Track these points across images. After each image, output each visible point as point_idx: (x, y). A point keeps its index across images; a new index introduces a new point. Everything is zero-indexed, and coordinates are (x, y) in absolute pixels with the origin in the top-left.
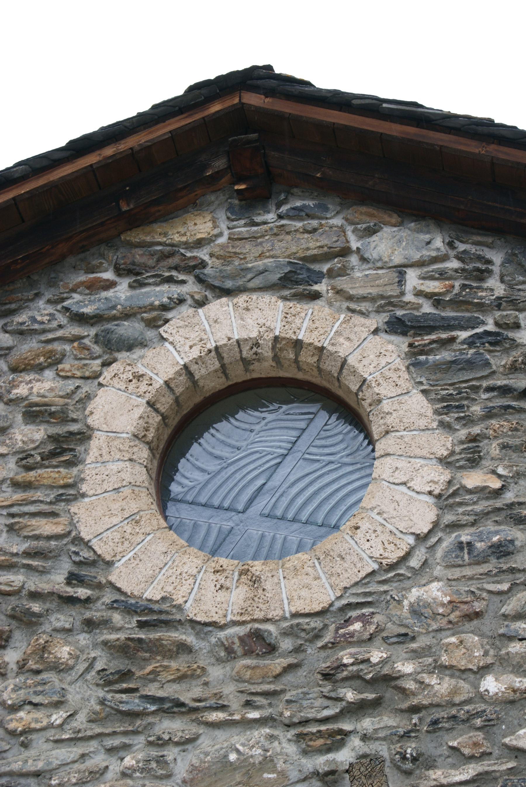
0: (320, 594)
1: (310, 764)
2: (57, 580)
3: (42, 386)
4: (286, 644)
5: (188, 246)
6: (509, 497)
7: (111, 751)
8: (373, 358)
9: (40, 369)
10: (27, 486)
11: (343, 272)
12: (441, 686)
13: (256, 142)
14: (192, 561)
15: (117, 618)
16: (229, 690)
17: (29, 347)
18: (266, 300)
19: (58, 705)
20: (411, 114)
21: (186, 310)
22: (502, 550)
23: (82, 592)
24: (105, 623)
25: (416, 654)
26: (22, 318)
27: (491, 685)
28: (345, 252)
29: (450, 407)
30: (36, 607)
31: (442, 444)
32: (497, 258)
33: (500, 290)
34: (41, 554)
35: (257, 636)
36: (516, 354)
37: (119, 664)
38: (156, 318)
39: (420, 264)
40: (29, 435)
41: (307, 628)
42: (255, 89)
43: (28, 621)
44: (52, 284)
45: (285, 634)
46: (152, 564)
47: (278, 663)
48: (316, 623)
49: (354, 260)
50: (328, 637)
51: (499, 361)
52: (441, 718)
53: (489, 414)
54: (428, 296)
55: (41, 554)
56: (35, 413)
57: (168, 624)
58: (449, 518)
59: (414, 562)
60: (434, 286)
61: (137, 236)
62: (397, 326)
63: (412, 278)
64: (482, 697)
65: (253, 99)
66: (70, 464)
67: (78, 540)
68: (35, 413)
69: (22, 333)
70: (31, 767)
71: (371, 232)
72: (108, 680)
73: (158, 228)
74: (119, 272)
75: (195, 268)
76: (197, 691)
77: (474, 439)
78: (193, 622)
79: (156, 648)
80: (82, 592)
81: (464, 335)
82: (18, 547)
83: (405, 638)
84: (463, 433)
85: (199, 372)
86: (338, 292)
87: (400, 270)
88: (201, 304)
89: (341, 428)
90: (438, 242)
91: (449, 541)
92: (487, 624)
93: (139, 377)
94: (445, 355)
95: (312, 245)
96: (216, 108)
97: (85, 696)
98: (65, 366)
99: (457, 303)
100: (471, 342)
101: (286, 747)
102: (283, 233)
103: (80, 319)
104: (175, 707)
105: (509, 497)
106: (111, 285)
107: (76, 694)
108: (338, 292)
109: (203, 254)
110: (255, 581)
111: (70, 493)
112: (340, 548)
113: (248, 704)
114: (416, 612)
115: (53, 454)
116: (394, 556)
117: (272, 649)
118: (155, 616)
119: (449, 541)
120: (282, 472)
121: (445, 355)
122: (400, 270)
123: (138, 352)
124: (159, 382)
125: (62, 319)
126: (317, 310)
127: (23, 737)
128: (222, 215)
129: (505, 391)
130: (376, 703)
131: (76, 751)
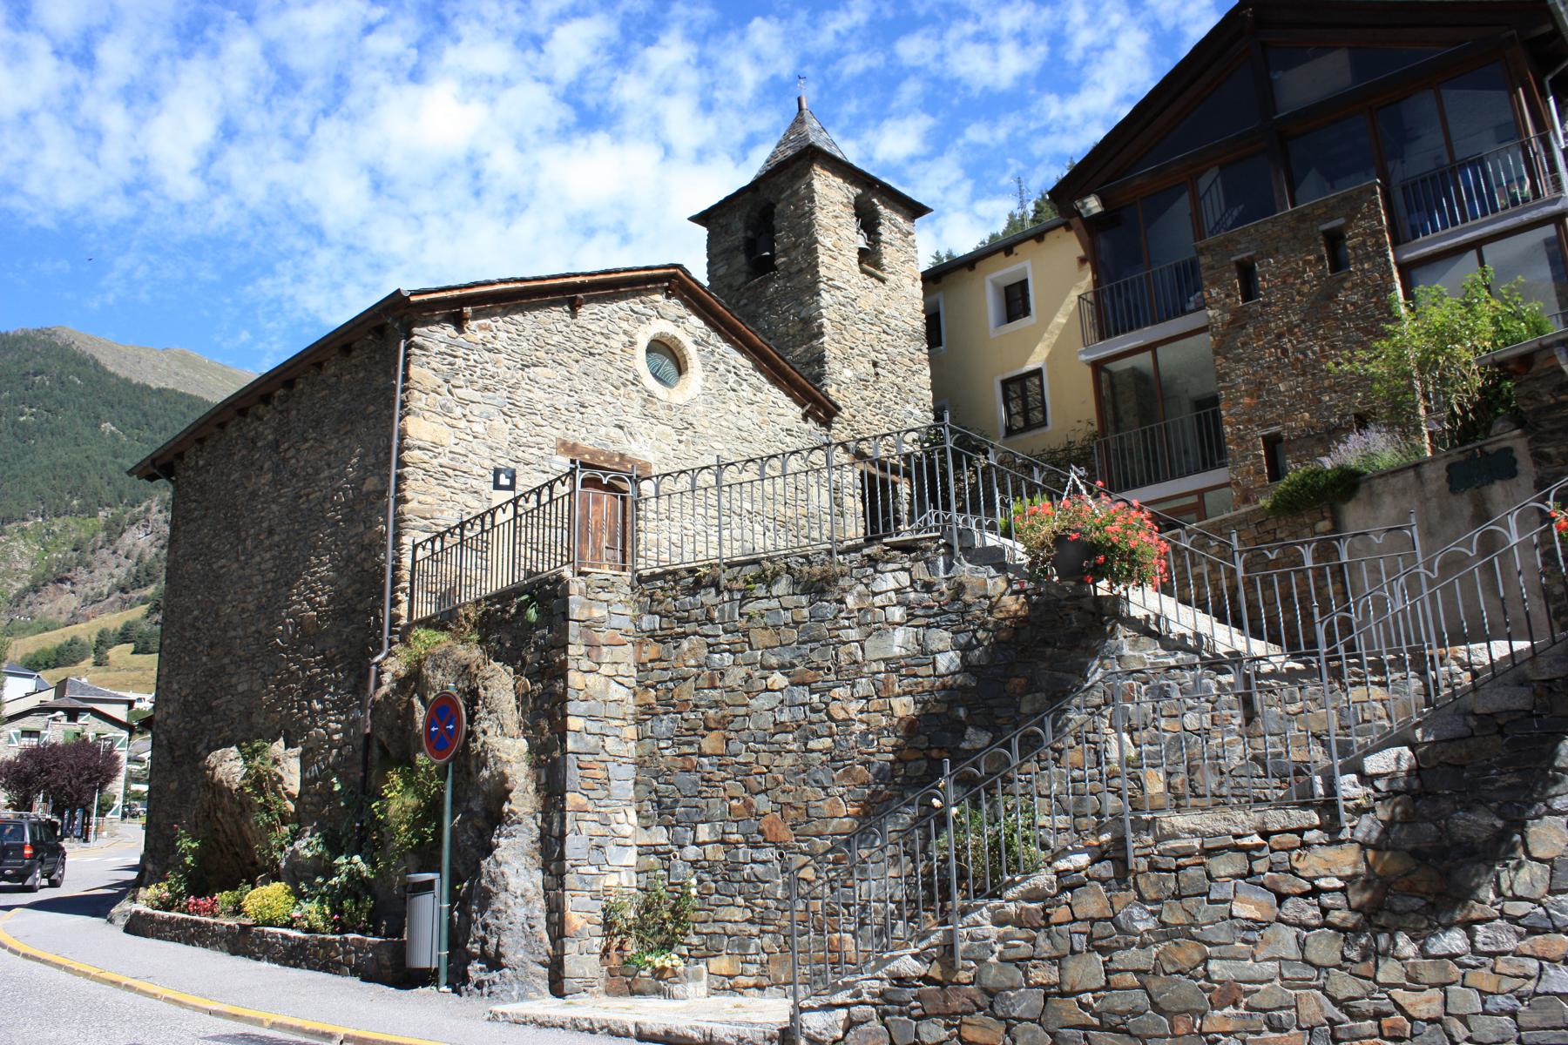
2: (631, 377)
8: (691, 350)
17: (622, 313)
29: (704, 365)
40: (626, 339)
55: (627, 370)
56: (625, 333)
62: (696, 342)
68: (625, 333)
97: (637, 409)
102: (674, 307)
104: (654, 417)
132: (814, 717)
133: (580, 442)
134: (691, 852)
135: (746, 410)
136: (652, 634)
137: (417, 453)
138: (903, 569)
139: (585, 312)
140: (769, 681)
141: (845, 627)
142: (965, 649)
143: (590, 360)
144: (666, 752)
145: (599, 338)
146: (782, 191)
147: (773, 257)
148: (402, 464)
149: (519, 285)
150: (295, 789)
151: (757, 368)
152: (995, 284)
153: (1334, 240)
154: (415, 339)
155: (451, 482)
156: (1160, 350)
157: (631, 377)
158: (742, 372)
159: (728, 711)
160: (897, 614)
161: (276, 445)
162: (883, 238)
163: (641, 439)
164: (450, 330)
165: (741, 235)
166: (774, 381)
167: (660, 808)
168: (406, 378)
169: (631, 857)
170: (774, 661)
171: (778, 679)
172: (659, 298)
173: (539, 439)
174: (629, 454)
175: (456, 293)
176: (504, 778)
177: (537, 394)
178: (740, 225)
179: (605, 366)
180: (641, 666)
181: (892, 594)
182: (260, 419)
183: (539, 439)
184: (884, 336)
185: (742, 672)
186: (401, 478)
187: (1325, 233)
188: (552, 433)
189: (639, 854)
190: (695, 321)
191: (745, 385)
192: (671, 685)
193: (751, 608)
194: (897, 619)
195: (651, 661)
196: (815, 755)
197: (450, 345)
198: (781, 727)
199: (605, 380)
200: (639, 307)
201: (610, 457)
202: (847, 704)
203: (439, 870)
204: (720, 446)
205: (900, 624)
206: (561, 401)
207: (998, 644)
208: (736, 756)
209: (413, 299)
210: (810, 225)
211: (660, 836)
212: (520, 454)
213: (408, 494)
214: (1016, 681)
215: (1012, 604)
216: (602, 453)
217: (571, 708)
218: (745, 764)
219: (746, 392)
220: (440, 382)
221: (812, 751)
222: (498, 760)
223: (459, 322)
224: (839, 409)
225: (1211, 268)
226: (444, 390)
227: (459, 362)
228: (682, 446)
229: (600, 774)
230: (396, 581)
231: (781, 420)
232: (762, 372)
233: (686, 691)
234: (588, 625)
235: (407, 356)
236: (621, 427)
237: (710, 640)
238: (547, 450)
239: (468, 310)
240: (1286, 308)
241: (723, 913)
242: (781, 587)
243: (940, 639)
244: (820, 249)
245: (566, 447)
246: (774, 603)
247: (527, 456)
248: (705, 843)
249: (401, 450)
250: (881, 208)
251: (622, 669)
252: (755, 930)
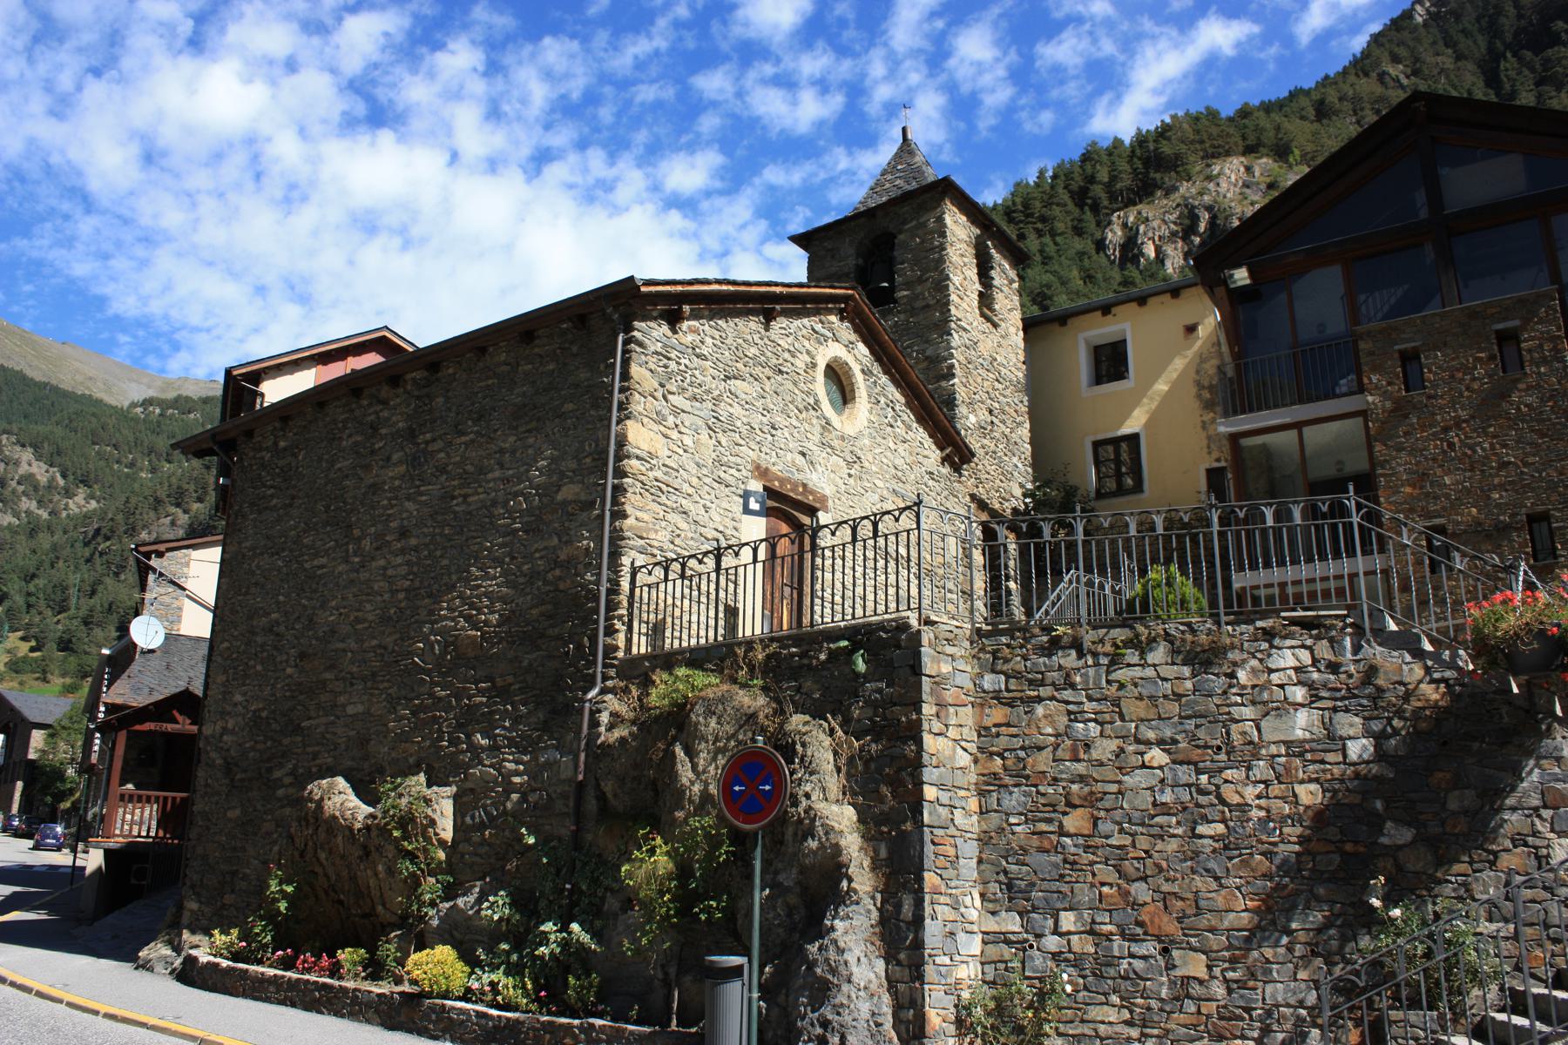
2: (812, 401)
8: (859, 378)
17: (804, 331)
40: (809, 360)
55: (808, 393)
56: (808, 352)
62: (863, 371)
68: (808, 352)
97: (816, 438)
132: (1203, 800)
134: (1052, 943)
135: (901, 448)
136: (997, 695)
137: (634, 462)
138: (1303, 646)
139: (780, 323)
140: (1147, 757)
141: (1237, 704)
142: (1379, 738)
143: (779, 378)
144: (1017, 829)
145: (786, 355)
146: (904, 223)
147: (892, 289)
148: (621, 473)
149: (731, 288)
150: (448, 835)
151: (908, 404)
152: (1087, 342)
153: (1507, 339)
154: (635, 333)
155: (663, 499)
156: (1307, 431)
157: (812, 401)
158: (897, 408)
159: (1099, 787)
160: (1299, 694)
161: (411, 434)
162: (996, 283)
164: (665, 329)
165: (852, 262)
166: (921, 420)
167: (1010, 891)
168: (626, 376)
169: (975, 946)
170: (1151, 735)
171: (1157, 756)
173: (739, 460)
174: (811, 485)
175: (680, 288)
176: (837, 850)
177: (737, 410)
178: (851, 251)
179: (791, 387)
180: (982, 731)
181: (1292, 672)
182: (385, 402)
183: (739, 460)
184: (997, 385)
185: (1113, 745)
186: (619, 490)
187: (1497, 332)
188: (749, 454)
189: (984, 942)
190: (862, 349)
192: (1022, 754)
193: (1121, 674)
194: (1299, 699)
195: (995, 725)
196: (1206, 841)
197: (665, 346)
198: (1165, 809)
200: (818, 327)
201: (795, 485)
202: (1242, 788)
203: (747, 952)
205: (1303, 705)
206: (757, 419)
207: (1417, 735)
208: (1107, 837)
209: (643, 289)
210: (941, 261)
211: (1011, 923)
212: (722, 475)
213: (629, 509)
214: (1440, 775)
215: (1432, 693)
216: (789, 480)
217: (929, 774)
218: (1118, 847)
220: (656, 385)
221: (1201, 837)
222: (829, 830)
223: (674, 319)
224: (973, 455)
225: (1371, 353)
226: (659, 395)
227: (673, 365)
228: (851, 481)
229: (951, 851)
230: (612, 606)
233: (1042, 761)
234: (939, 681)
235: (625, 352)
236: (804, 455)
237: (1071, 707)
239: (686, 308)
240: (1453, 403)
241: (1094, 1013)
242: (1158, 655)
243: (1349, 724)
244: (952, 288)
246: (1150, 672)
248: (1069, 933)
249: (619, 457)
250: (993, 251)
251: (965, 730)
252: (1135, 1033)
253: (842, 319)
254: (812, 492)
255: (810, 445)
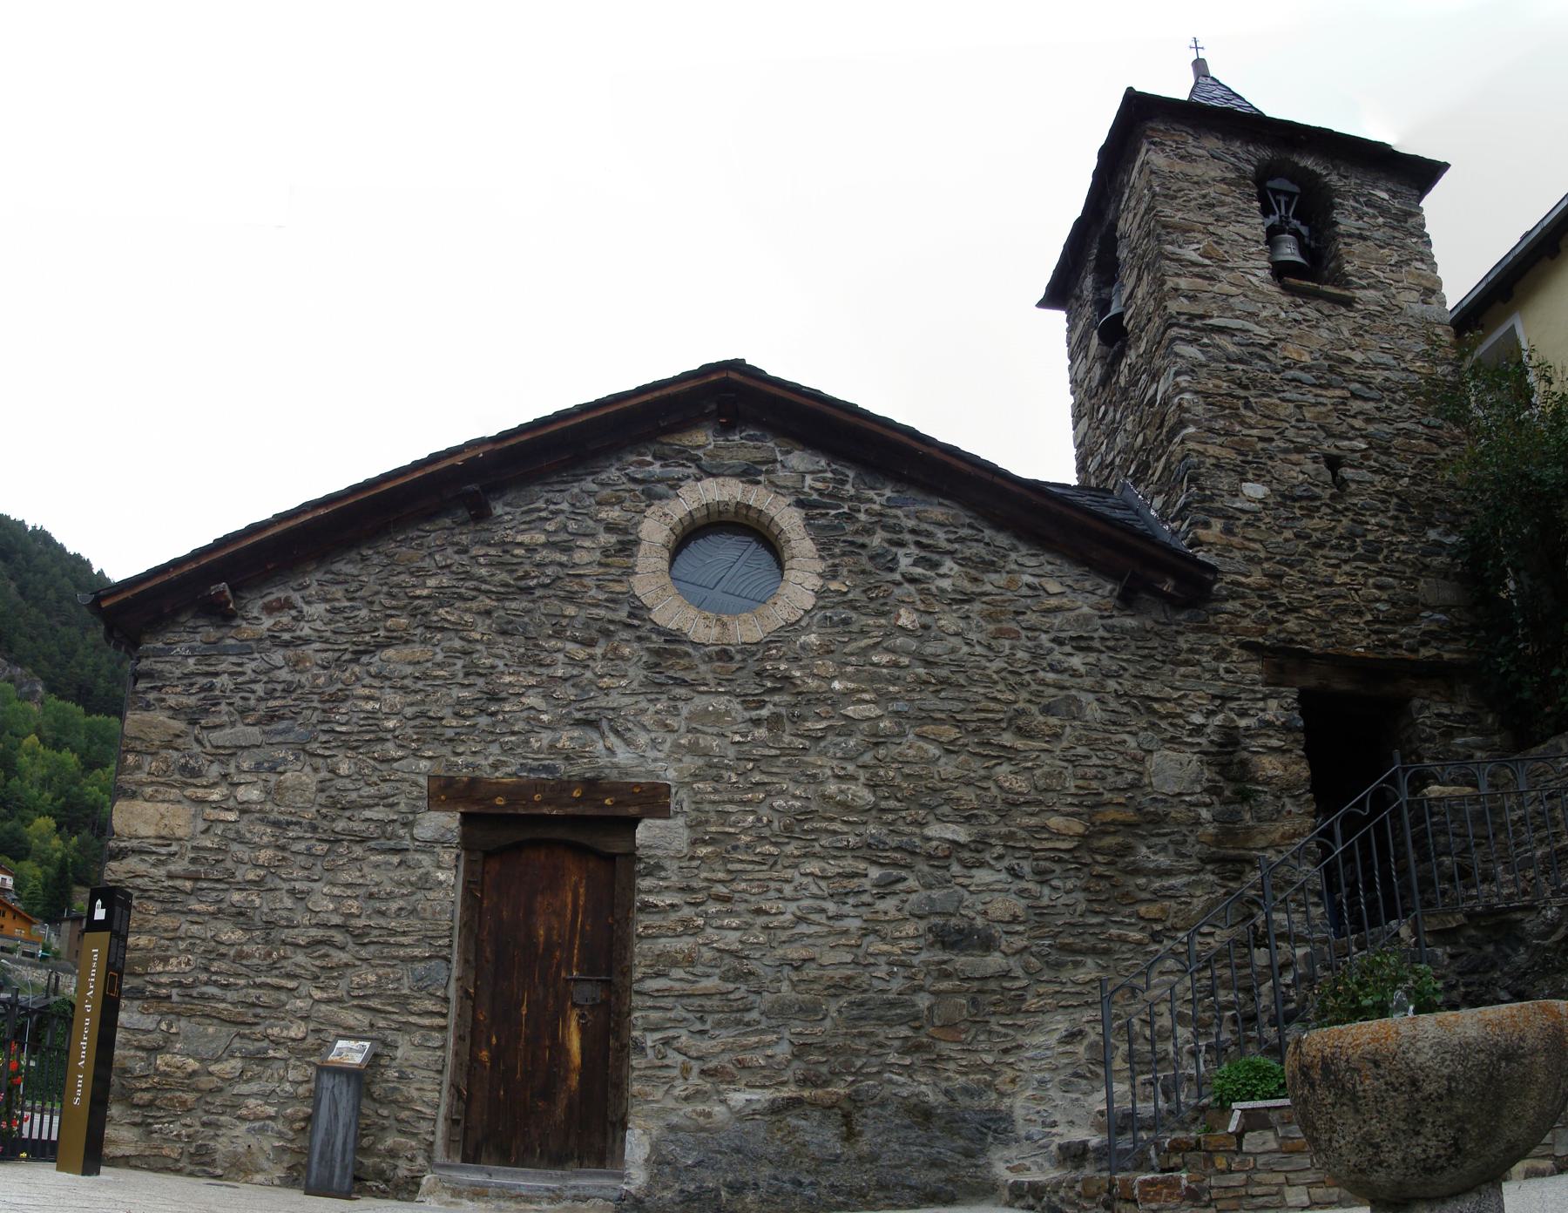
0: (756, 634)
1: (747, 715)
2: (622, 614)
3: (613, 514)
4: (738, 657)
5: (692, 447)
6: (850, 596)
7: (650, 701)
8: (788, 519)
9: (612, 504)
10: (607, 565)
11: (773, 472)
12: (813, 684)
13: (733, 401)
14: (692, 612)
15: (654, 636)
16: (709, 676)
17: (606, 492)
18: (733, 482)
19: (624, 676)
20: (816, 396)
21: (690, 482)
22: (846, 622)
23: (636, 622)
24: (648, 639)
25: (801, 668)
26: (603, 476)
27: (836, 685)
28: (775, 461)
29: (824, 548)
30: (612, 628)
31: (820, 566)
32: (851, 474)
33: (852, 492)
34: (613, 601)
35: (725, 651)
36: (857, 525)
37: (653, 660)
38: (675, 484)
39: (812, 473)
41: (748, 650)
42: (734, 370)
43: (608, 634)
44: (619, 459)
45: (740, 652)
46: (671, 612)
47: (734, 666)
48: (754, 648)
49: (779, 466)
50: (759, 656)
51: (849, 528)
52: (814, 698)
53: (844, 554)
54: (817, 490)
55: (613, 601)
56: (610, 528)
57: (679, 642)
58: (821, 603)
59: (803, 623)
60: (819, 485)
61: (665, 440)
62: (800, 504)
63: (809, 480)
64: (832, 690)
65: (733, 376)
66: (629, 556)
67: (634, 596)
68: (610, 528)
69: (603, 484)
70: (610, 705)
71: (788, 452)
72: (648, 666)
73: (677, 436)
74: (655, 457)
75: (696, 460)
76: (693, 676)
77: (835, 565)
78: (692, 643)
79: (674, 653)
80: (636, 622)
81: (833, 512)
82: (602, 596)
83: (797, 659)
84: (830, 562)
85: (697, 515)
86: (771, 482)
87: (803, 475)
88: (699, 480)
89: (765, 556)
90: (823, 463)
91: (820, 614)
92: (836, 656)
93: (666, 515)
94: (821, 522)
95: (759, 456)
96: (714, 378)
97: (636, 673)
98: (627, 504)
99: (830, 496)
100: (836, 516)
101: (736, 705)
102: (742, 446)
103: (634, 480)
104: (682, 683)
105: (850, 596)
106: (651, 464)
107: (631, 673)
108: (771, 482)
109: (700, 453)
110: (724, 625)
111: (629, 571)
112: (767, 613)
113: (719, 684)
114: (803, 647)
115: (620, 551)
116: (793, 619)
117: (731, 659)
118: (674, 637)
119: (820, 614)
120: (733, 571)
121: (821, 522)
122: (803, 475)
123: (664, 502)
124: (676, 519)
125: (624, 479)
126: (755, 489)
127: (606, 691)
128: (710, 433)
129: (852, 543)
130: (780, 689)
131: (633, 699)
133: (486, 772)
135: (949, 621)
157: (622, 614)
163: (643, 739)
172: (703, 439)
173: (386, 788)
179: (554, 605)
183: (386, 788)
191: (948, 565)
199: (558, 634)
204: (875, 711)
216: (538, 785)
219: (950, 576)
228: (761, 732)
231: (1057, 621)
232: (999, 527)
238: (402, 807)
245: (444, 792)
247: (356, 826)
253: (725, 429)
254: (616, 789)
255: (615, 700)
